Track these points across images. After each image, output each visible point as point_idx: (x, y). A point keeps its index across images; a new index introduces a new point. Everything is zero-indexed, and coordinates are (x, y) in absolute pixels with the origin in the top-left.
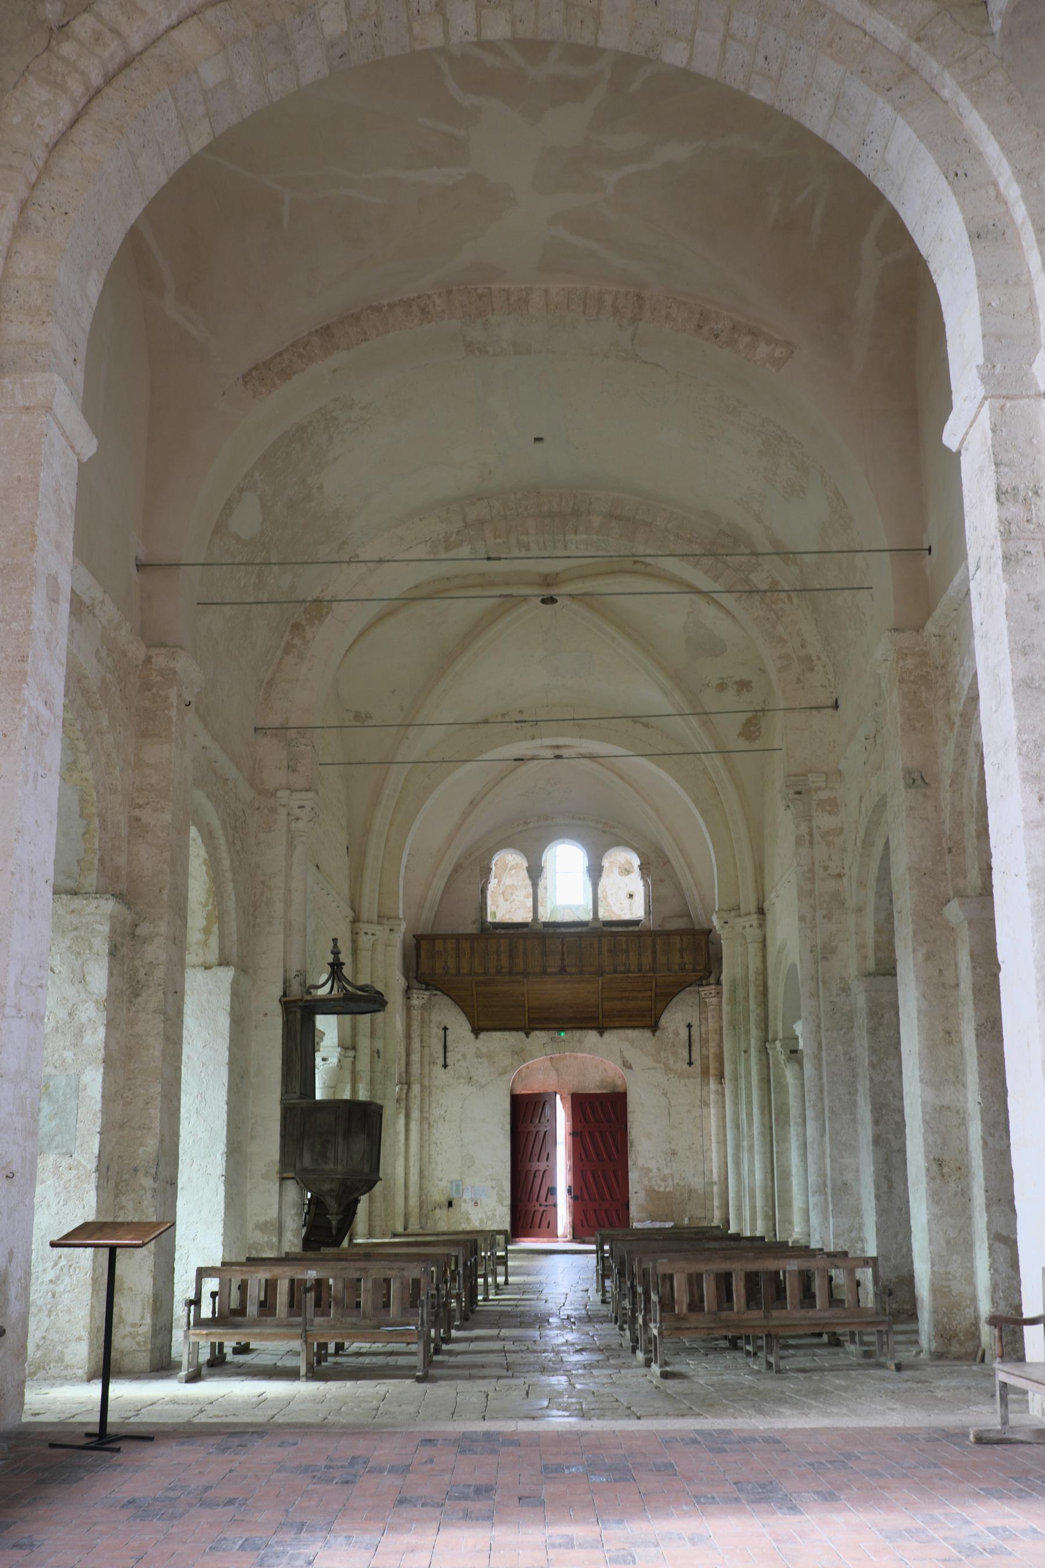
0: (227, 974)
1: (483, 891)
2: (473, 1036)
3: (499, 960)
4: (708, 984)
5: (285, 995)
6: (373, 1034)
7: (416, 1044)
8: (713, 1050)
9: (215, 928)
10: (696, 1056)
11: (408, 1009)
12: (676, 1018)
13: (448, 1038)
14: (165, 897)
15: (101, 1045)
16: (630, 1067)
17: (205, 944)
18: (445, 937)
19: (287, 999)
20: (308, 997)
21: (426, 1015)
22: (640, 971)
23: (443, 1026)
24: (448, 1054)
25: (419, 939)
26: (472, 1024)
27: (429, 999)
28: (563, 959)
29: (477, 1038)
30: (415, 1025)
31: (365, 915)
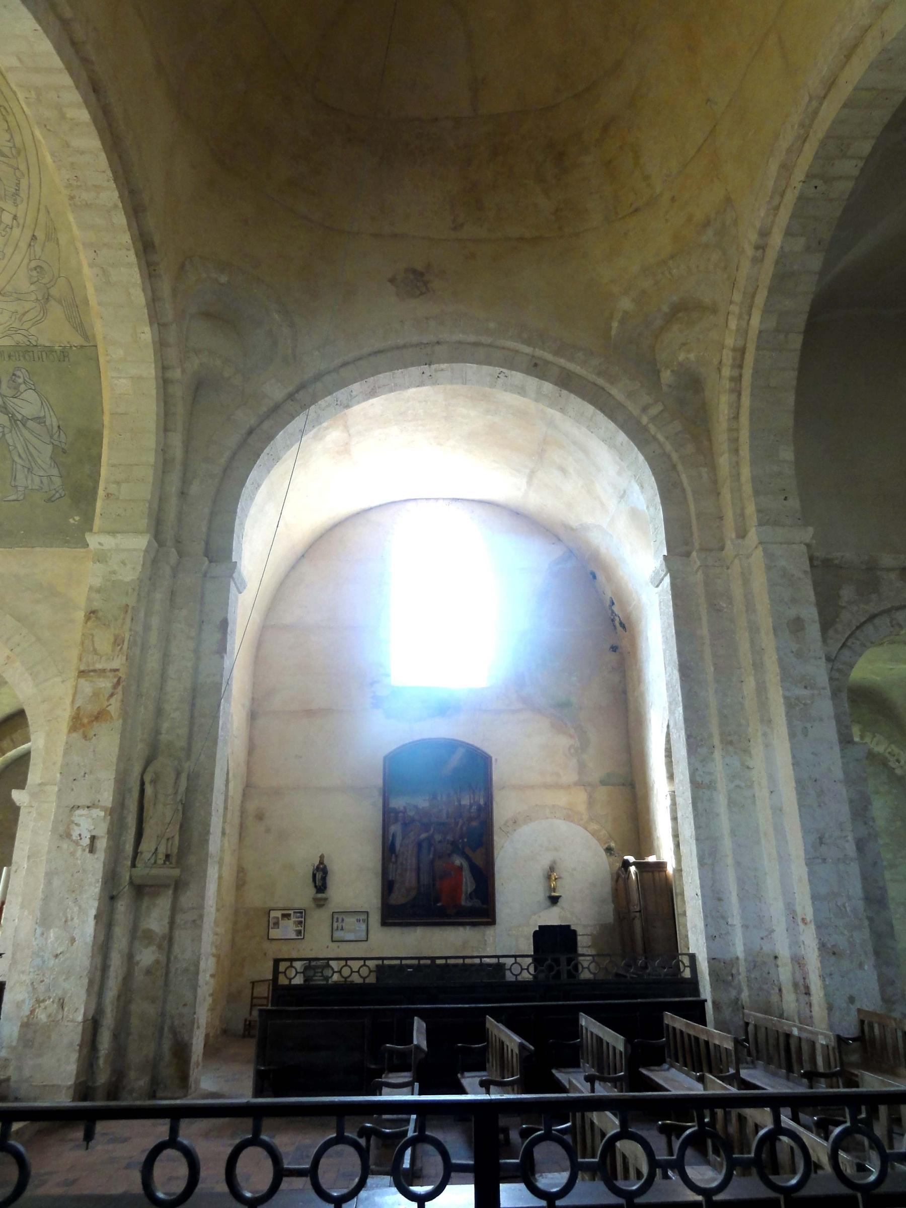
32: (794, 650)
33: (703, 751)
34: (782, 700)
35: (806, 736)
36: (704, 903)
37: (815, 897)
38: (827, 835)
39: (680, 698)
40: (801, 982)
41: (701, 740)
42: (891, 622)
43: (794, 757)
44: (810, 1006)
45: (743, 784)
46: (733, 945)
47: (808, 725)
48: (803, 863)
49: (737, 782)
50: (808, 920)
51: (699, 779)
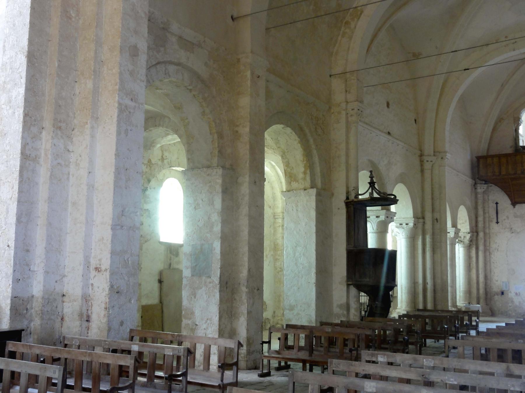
0: (314, 191)
1: (517, 130)
2: (512, 207)
5: (347, 198)
6: (433, 211)
7: (480, 212)
9: (308, 172)
13: (498, 208)
14: (248, 165)
15: (220, 231)
17: (304, 179)
18: (493, 157)
19: (349, 201)
20: (356, 200)
21: (486, 197)
25: (479, 158)
26: (511, 200)
27: (488, 188)
29: (514, 207)
30: (480, 202)
31: (426, 152)
32: (130, 70)
33: (34, 130)
34: (116, 105)
35: (127, 136)
36: (15, 253)
37: (113, 253)
38: (127, 210)
39: (23, 81)
40: (85, 313)
41: (35, 120)
42: (165, 71)
43: (117, 150)
44: (88, 329)
45: (63, 163)
46: (32, 286)
47: (129, 128)
48: (110, 227)
49: (60, 161)
50: (103, 268)
51: (28, 152)
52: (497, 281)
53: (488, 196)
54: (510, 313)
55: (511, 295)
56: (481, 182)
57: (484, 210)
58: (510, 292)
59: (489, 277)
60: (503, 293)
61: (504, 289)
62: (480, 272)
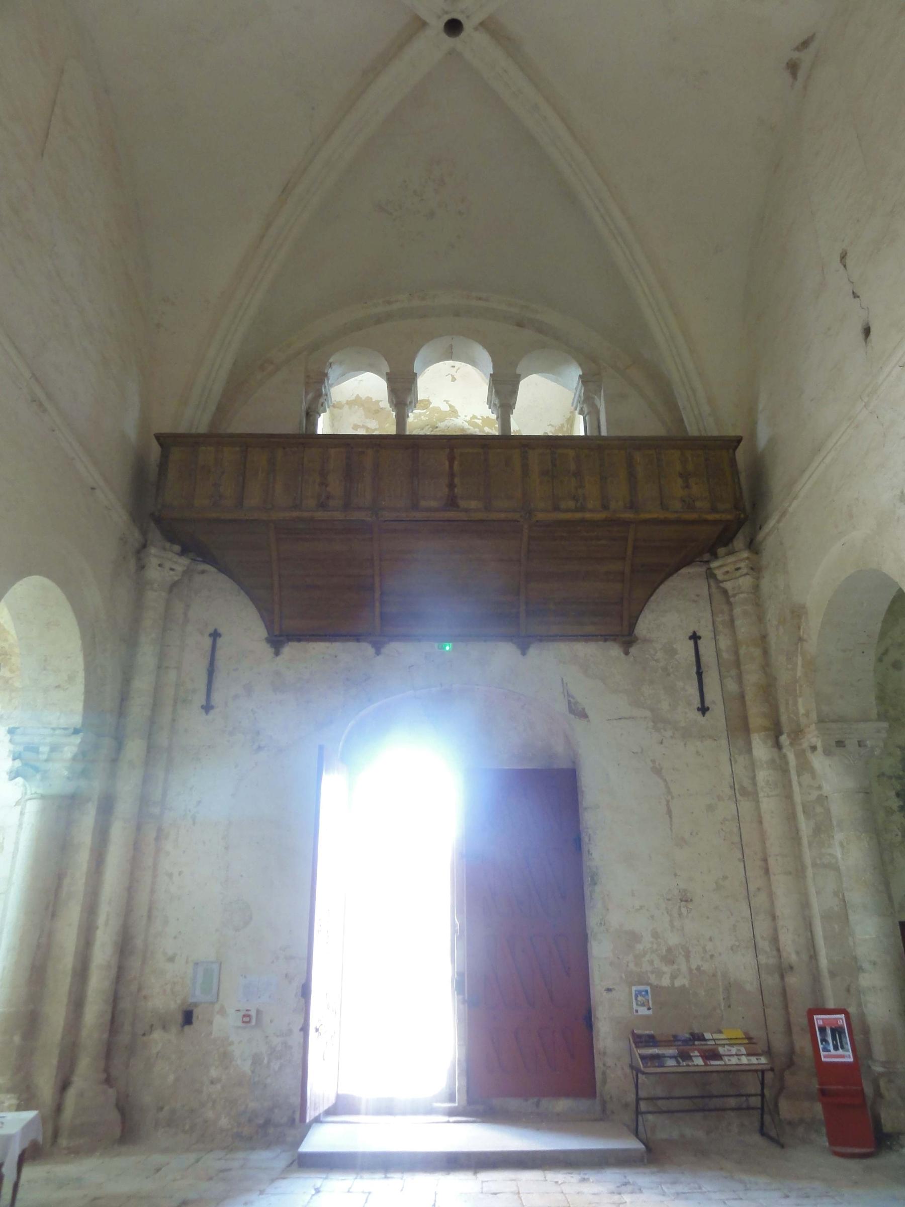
2: (268, 650)
3: (324, 484)
4: (731, 553)
8: (753, 677)
10: (713, 694)
11: (140, 586)
12: (673, 616)
13: (219, 654)
16: (583, 715)
22: (605, 507)
23: (211, 630)
24: (217, 684)
25: (166, 441)
26: (269, 626)
27: (188, 573)
28: (451, 486)
29: (277, 653)
52: (171, 959)
53: (188, 606)
54: (210, 1114)
55: (223, 1023)
56: (168, 545)
57: (162, 656)
58: (222, 1012)
59: (139, 942)
60: (188, 1017)
61: (199, 996)
62: (101, 920)
